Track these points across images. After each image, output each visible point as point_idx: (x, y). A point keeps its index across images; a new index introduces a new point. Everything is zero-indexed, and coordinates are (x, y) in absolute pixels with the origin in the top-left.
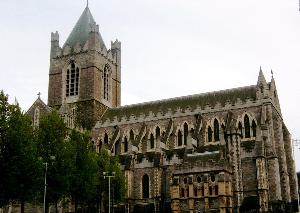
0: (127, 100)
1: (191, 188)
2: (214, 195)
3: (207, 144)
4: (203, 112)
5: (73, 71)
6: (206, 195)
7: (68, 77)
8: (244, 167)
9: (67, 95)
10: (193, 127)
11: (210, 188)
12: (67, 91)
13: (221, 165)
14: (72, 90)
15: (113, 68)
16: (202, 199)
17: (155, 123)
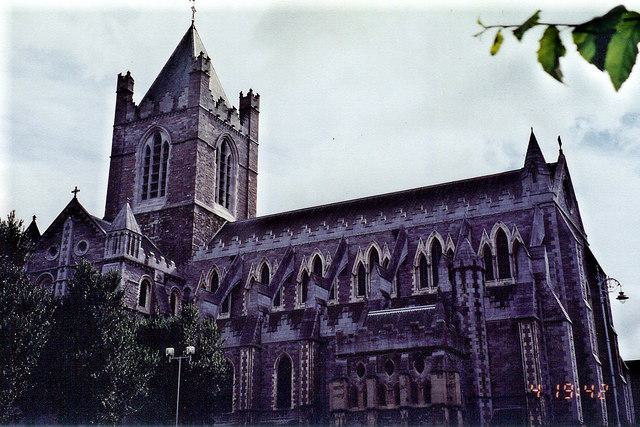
1: (371, 385)
2: (422, 405)
3: (416, 292)
4: (408, 225)
5: (157, 150)
6: (403, 403)
7: (147, 160)
8: (494, 344)
9: (144, 197)
10: (388, 255)
11: (414, 387)
12: (145, 188)
13: (437, 333)
14: (154, 187)
15: (240, 145)
16: (396, 413)
17: (314, 246)
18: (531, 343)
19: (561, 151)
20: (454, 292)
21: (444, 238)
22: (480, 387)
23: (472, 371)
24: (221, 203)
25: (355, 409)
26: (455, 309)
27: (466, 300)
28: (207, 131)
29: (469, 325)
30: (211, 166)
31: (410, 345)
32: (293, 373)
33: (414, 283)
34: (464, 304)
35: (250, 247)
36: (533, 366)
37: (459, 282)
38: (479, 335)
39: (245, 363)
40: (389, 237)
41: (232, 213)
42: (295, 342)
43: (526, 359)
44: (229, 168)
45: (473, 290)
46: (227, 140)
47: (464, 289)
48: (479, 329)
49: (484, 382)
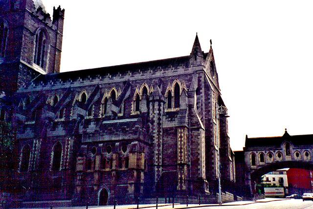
0: (64, 68)
1: (98, 158)
3: (133, 113)
4: (131, 79)
6: (114, 168)
8: (165, 139)
13: (135, 133)
15: (51, 35)
17: (83, 90)
18: (183, 139)
19: (211, 47)
20: (148, 113)
21: (149, 87)
22: (157, 160)
23: (153, 152)
24: (38, 64)
25: (89, 171)
26: (148, 121)
27: (154, 117)
28: (30, 23)
29: (154, 129)
30: (32, 43)
31: (121, 138)
32: (62, 152)
33: (132, 109)
34: (152, 119)
35: (48, 87)
36: (183, 150)
37: (151, 107)
38: (159, 135)
39: (35, 147)
40: (121, 84)
41: (45, 70)
42: (65, 136)
43: (179, 147)
44: (44, 46)
45: (158, 112)
46: (43, 31)
47: (153, 111)
48: (159, 131)
49: (158, 158)
